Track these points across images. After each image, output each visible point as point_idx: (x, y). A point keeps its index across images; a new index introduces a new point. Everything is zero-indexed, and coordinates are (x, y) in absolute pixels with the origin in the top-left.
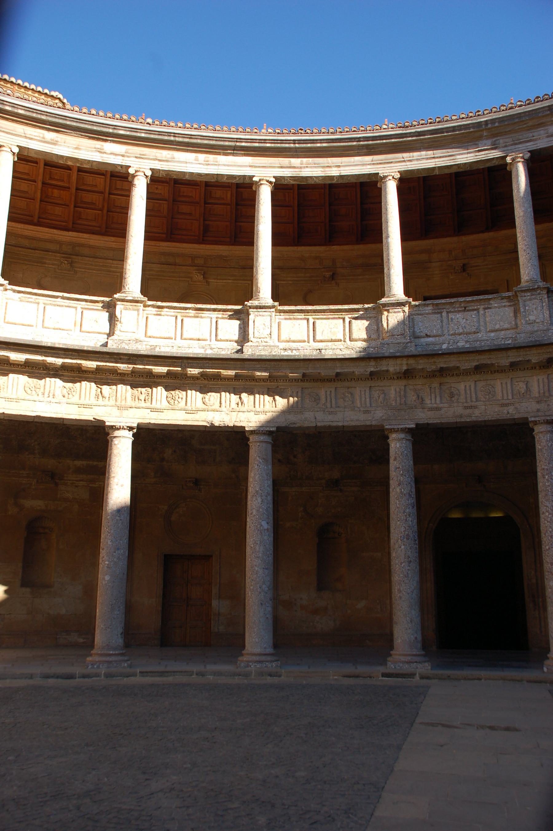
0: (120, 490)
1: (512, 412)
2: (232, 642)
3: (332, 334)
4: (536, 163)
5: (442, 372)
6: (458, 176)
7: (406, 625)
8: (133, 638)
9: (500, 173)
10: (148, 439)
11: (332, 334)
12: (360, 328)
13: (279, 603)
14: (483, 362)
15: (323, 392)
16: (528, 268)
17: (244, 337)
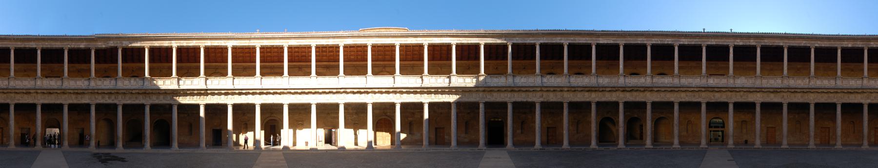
0: (426, 116)
1: (504, 100)
2: (449, 144)
3: (468, 81)
4: (513, 46)
5: (491, 91)
6: (497, 46)
7: (482, 141)
8: (430, 143)
9: (505, 47)
10: (432, 105)
11: (468, 81)
12: (475, 80)
13: (458, 136)
14: (500, 89)
15: (467, 94)
16: (509, 70)
17: (450, 82)
